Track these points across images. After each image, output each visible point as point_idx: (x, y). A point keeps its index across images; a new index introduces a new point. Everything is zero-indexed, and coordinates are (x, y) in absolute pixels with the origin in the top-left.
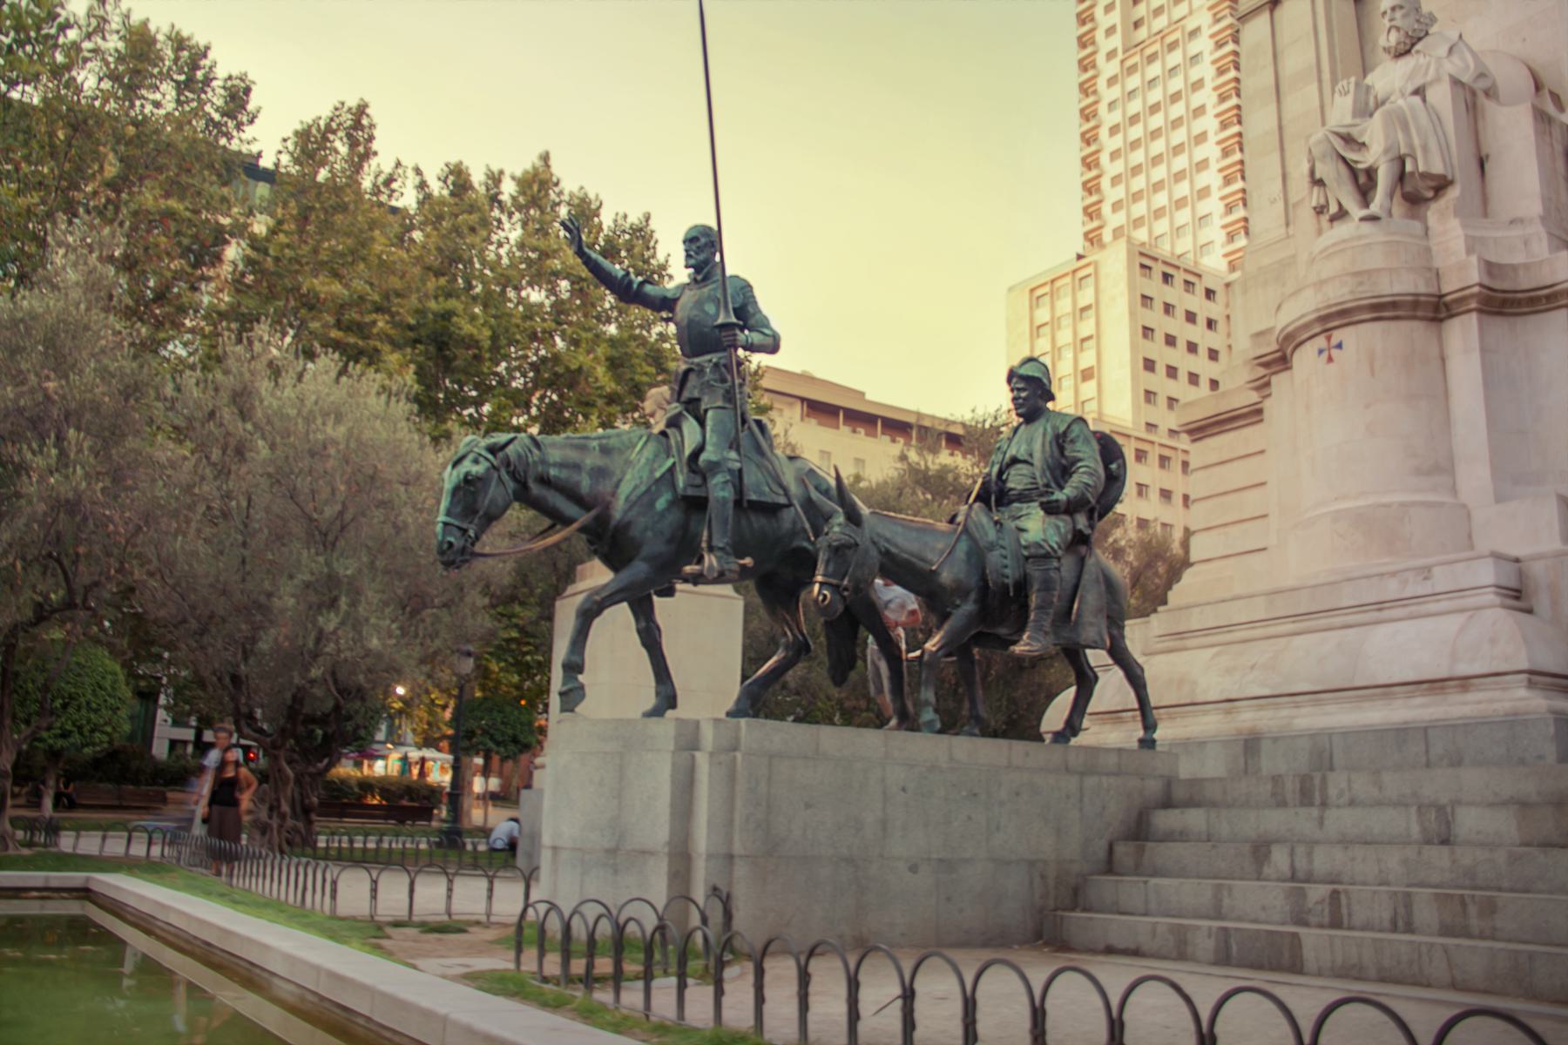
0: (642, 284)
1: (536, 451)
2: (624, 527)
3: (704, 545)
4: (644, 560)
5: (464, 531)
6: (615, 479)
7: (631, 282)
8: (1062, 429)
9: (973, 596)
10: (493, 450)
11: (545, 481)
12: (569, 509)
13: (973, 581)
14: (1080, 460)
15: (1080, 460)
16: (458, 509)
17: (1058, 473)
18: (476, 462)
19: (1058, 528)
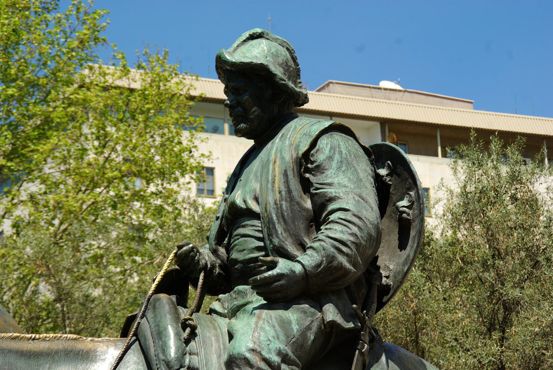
8: (304, 148)
14: (331, 200)
15: (331, 200)
17: (301, 225)
19: (285, 325)
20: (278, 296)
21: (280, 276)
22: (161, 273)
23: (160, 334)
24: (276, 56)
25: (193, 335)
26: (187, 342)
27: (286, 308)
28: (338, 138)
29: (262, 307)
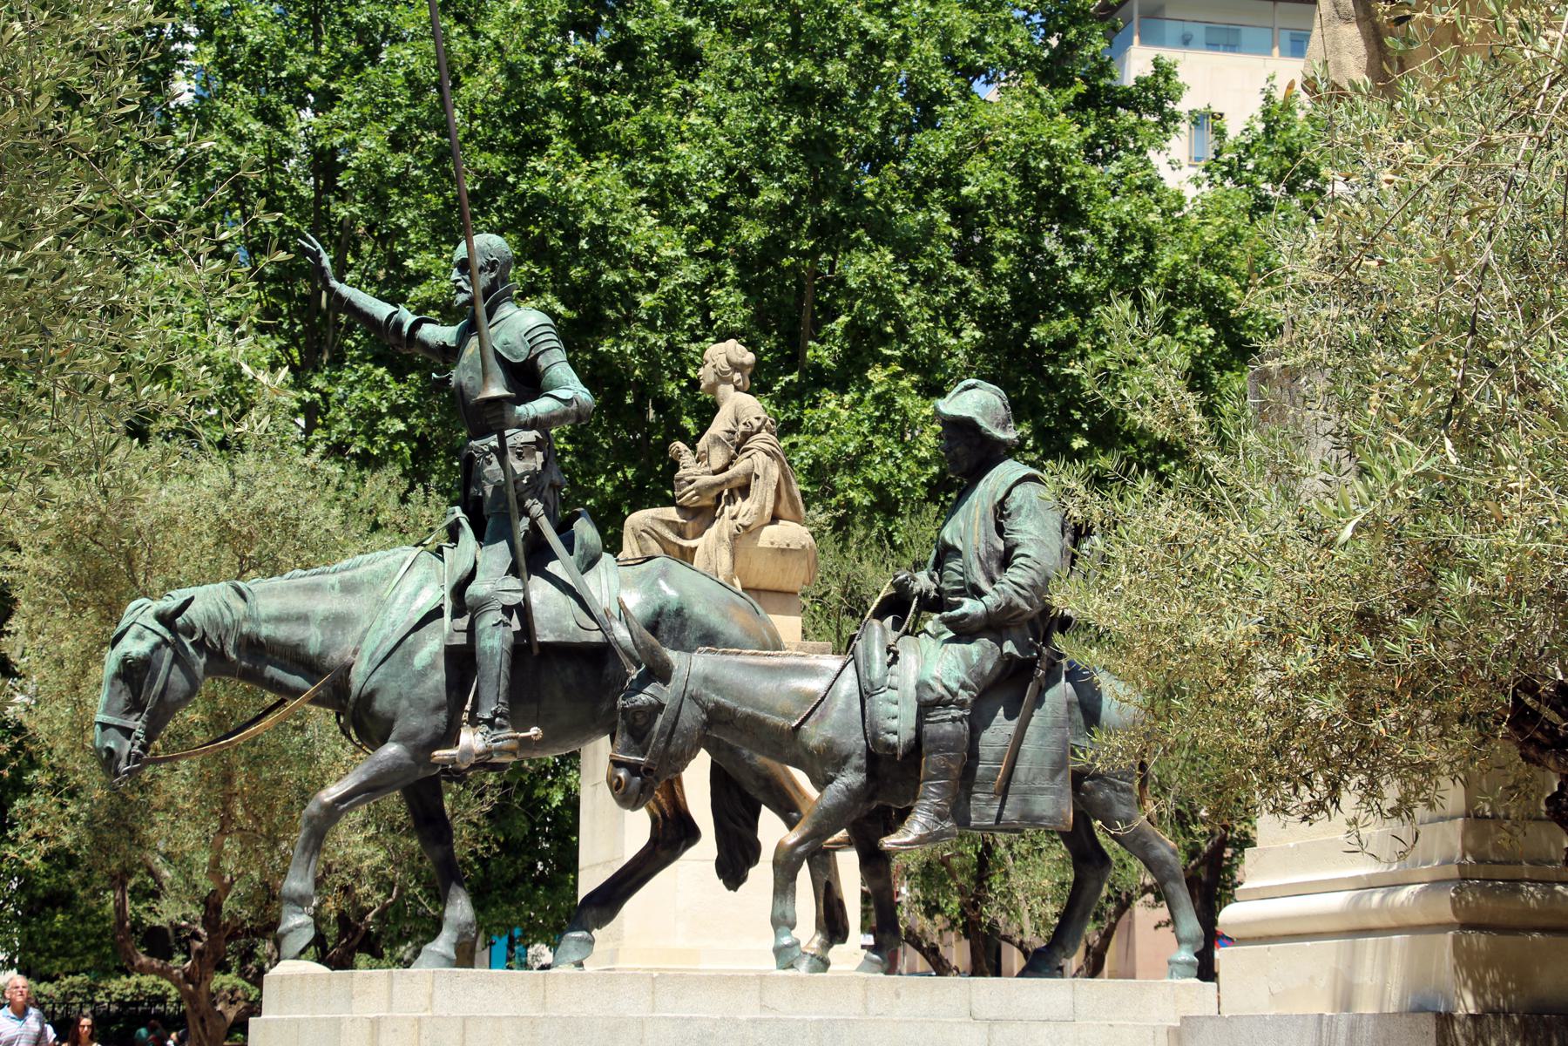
0: (416, 325)
1: (238, 605)
2: (368, 698)
3: (465, 716)
4: (401, 740)
5: (127, 732)
6: (360, 629)
7: (399, 325)
8: (1000, 496)
9: (857, 761)
10: (166, 619)
11: (255, 647)
12: (296, 681)
13: (855, 741)
14: (1017, 545)
15: (1017, 545)
16: (120, 702)
17: (994, 565)
18: (140, 637)
19: (966, 656)
20: (964, 631)
21: (965, 615)
22: (878, 600)
23: (868, 657)
24: (985, 408)
25: (895, 659)
26: (889, 665)
27: (970, 642)
28: (1030, 487)
29: (949, 641)
